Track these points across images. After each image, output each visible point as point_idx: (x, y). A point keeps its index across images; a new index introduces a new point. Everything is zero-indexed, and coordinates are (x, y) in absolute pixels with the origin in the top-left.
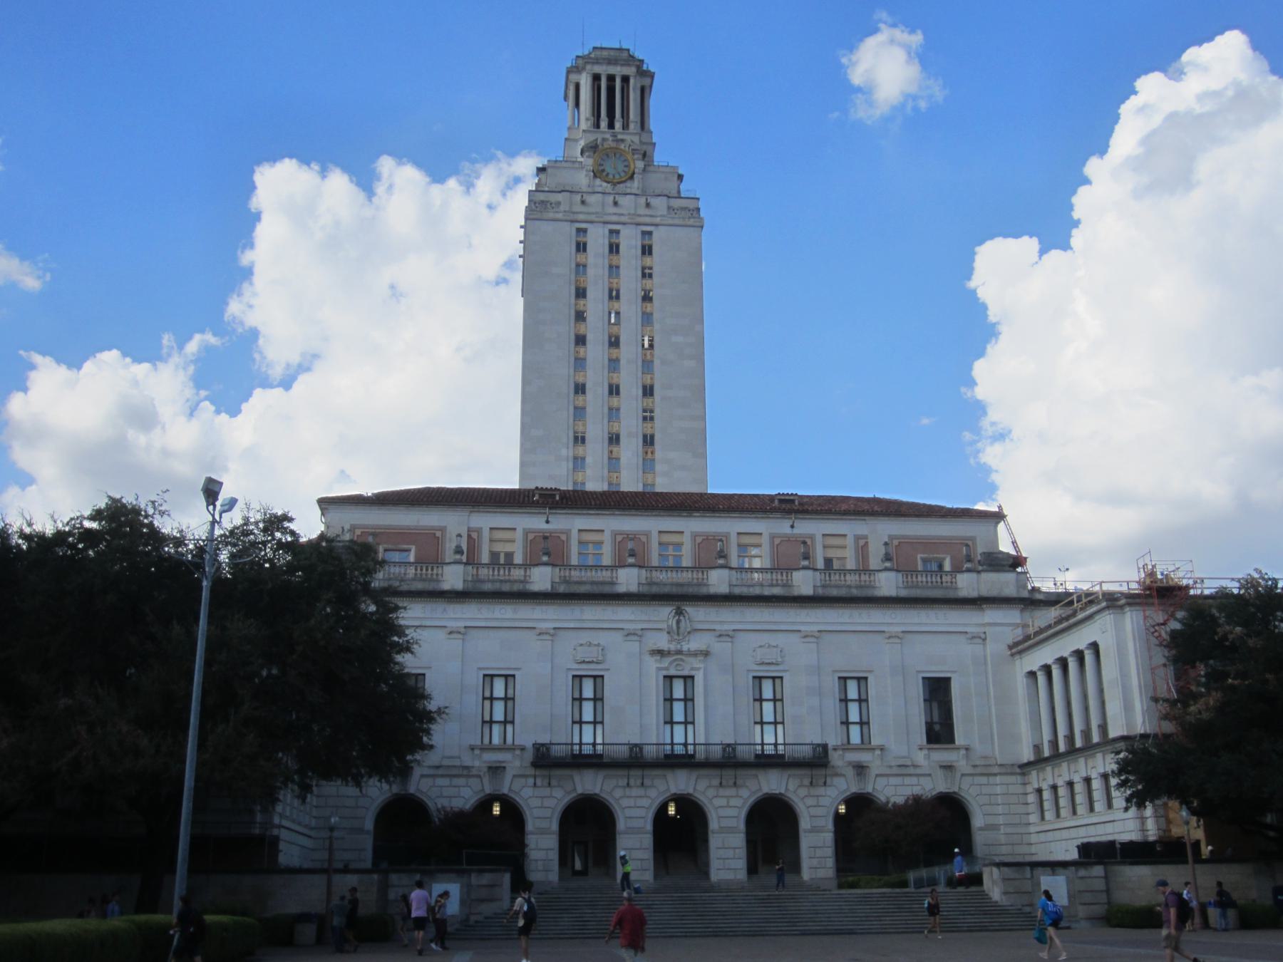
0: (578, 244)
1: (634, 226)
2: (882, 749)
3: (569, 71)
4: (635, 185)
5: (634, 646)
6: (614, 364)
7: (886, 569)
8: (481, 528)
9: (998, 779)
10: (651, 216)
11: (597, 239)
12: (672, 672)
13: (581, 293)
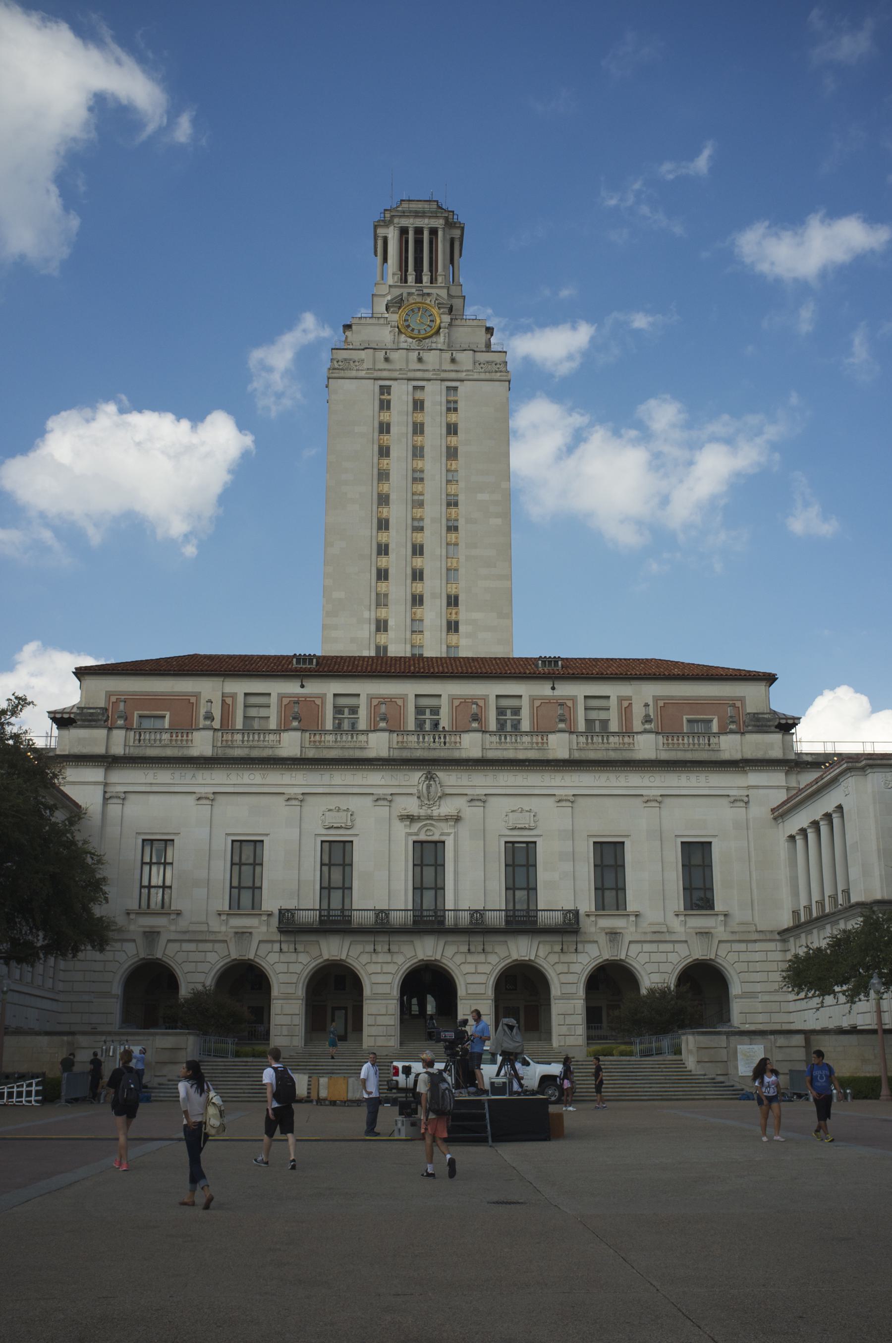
0: (381, 402)
1: (440, 381)
2: (637, 916)
5: (383, 811)
7: (646, 731)
8: (236, 694)
9: (758, 946)
10: (457, 371)
12: (422, 837)
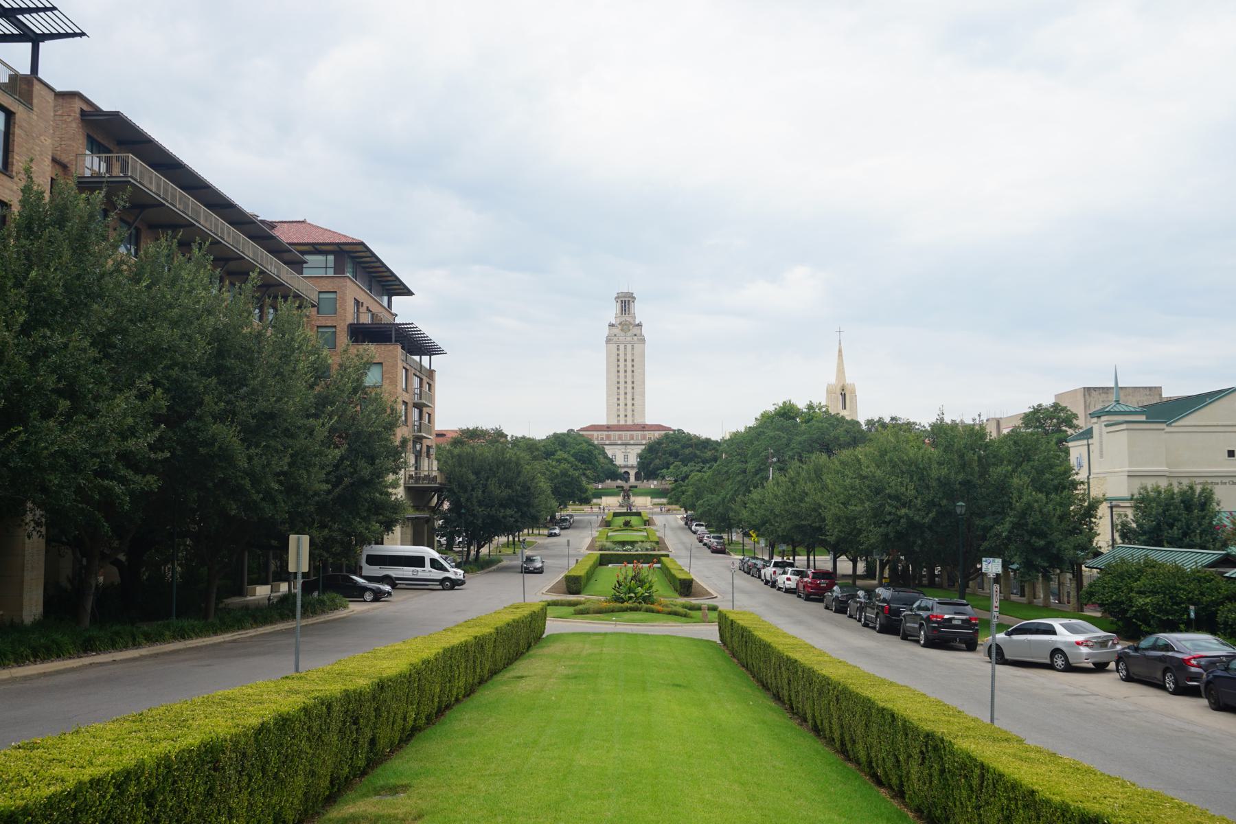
3: (616, 298)
4: (629, 334)
6: (626, 377)
11: (622, 347)
13: (618, 360)
